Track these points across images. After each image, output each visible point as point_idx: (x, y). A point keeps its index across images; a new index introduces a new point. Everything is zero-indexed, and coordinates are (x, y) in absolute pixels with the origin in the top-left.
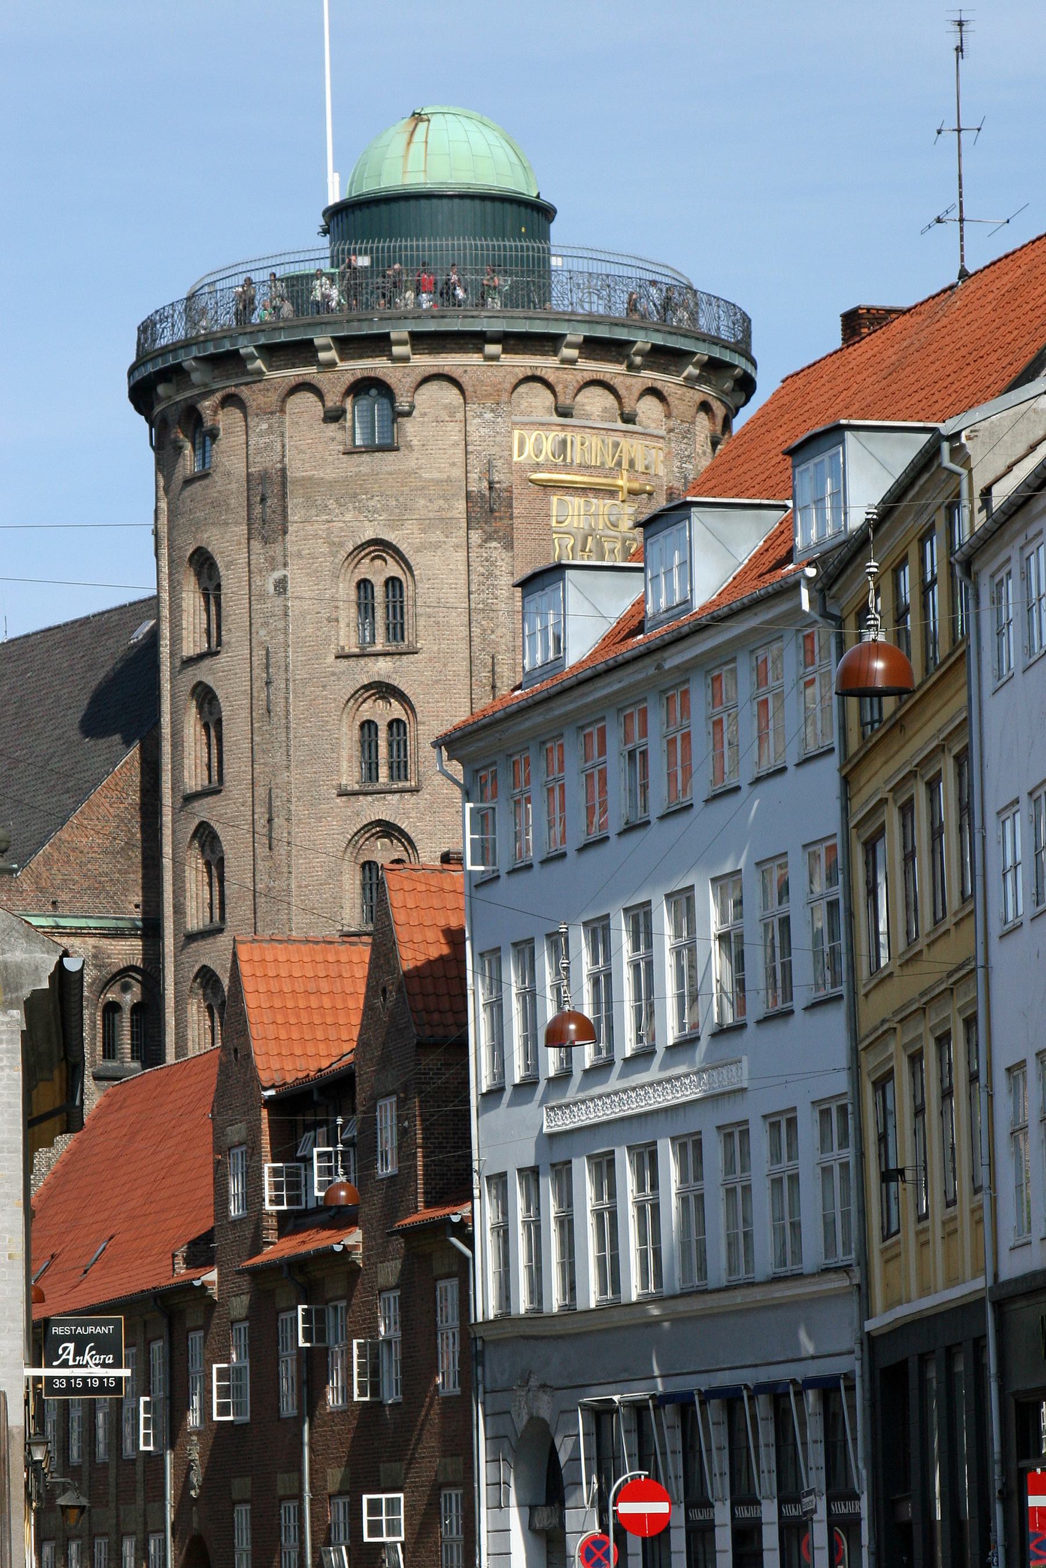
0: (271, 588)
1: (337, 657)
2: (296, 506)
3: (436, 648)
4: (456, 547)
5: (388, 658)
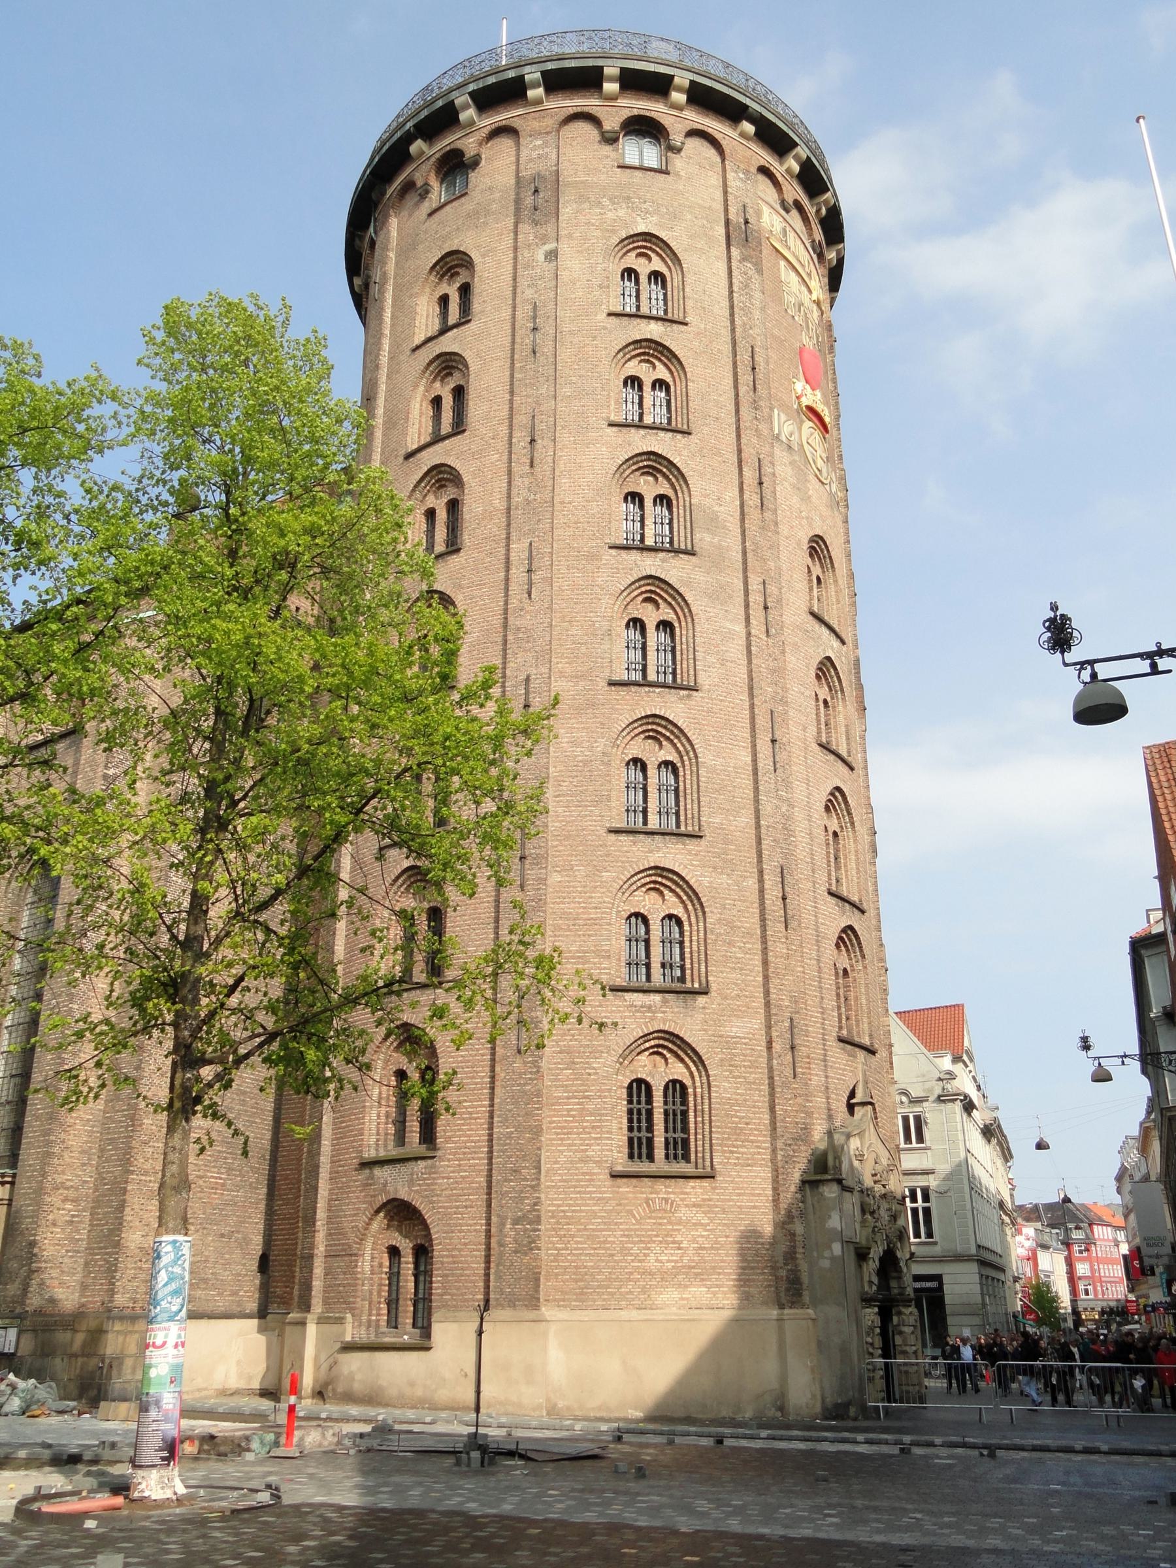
0: (541, 257)
1: (610, 315)
2: (568, 202)
3: (703, 326)
4: (718, 258)
5: (660, 323)
